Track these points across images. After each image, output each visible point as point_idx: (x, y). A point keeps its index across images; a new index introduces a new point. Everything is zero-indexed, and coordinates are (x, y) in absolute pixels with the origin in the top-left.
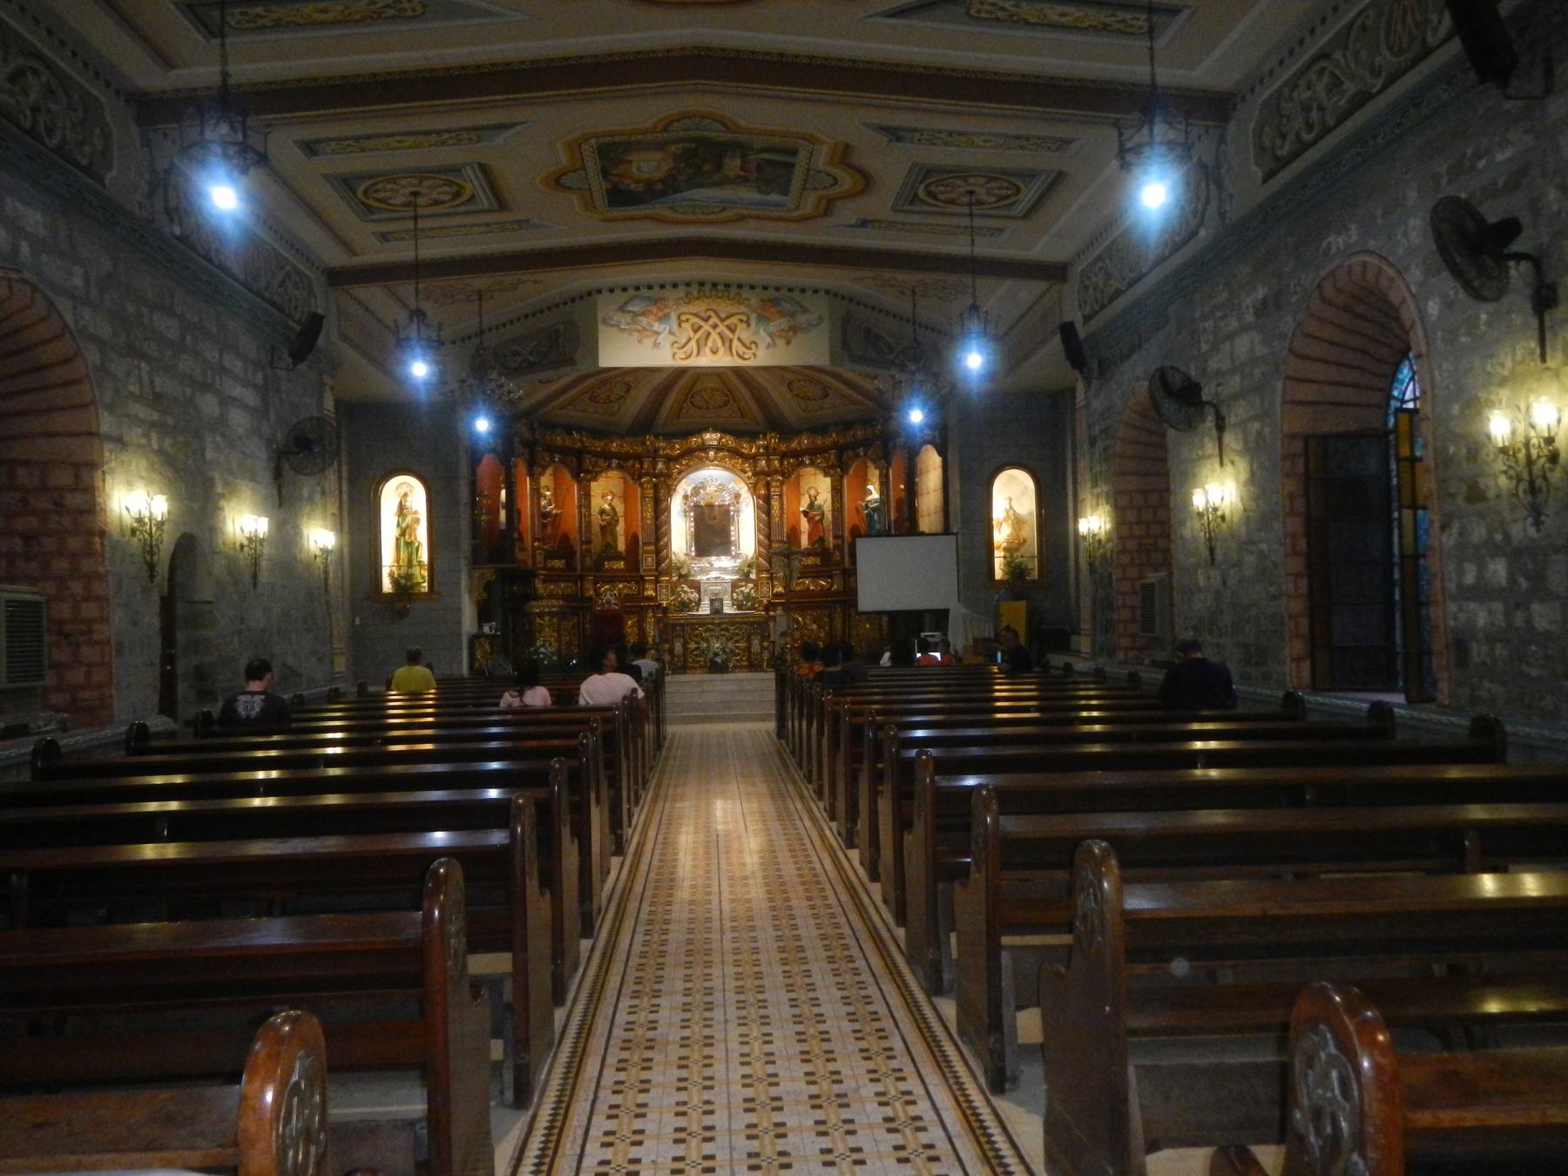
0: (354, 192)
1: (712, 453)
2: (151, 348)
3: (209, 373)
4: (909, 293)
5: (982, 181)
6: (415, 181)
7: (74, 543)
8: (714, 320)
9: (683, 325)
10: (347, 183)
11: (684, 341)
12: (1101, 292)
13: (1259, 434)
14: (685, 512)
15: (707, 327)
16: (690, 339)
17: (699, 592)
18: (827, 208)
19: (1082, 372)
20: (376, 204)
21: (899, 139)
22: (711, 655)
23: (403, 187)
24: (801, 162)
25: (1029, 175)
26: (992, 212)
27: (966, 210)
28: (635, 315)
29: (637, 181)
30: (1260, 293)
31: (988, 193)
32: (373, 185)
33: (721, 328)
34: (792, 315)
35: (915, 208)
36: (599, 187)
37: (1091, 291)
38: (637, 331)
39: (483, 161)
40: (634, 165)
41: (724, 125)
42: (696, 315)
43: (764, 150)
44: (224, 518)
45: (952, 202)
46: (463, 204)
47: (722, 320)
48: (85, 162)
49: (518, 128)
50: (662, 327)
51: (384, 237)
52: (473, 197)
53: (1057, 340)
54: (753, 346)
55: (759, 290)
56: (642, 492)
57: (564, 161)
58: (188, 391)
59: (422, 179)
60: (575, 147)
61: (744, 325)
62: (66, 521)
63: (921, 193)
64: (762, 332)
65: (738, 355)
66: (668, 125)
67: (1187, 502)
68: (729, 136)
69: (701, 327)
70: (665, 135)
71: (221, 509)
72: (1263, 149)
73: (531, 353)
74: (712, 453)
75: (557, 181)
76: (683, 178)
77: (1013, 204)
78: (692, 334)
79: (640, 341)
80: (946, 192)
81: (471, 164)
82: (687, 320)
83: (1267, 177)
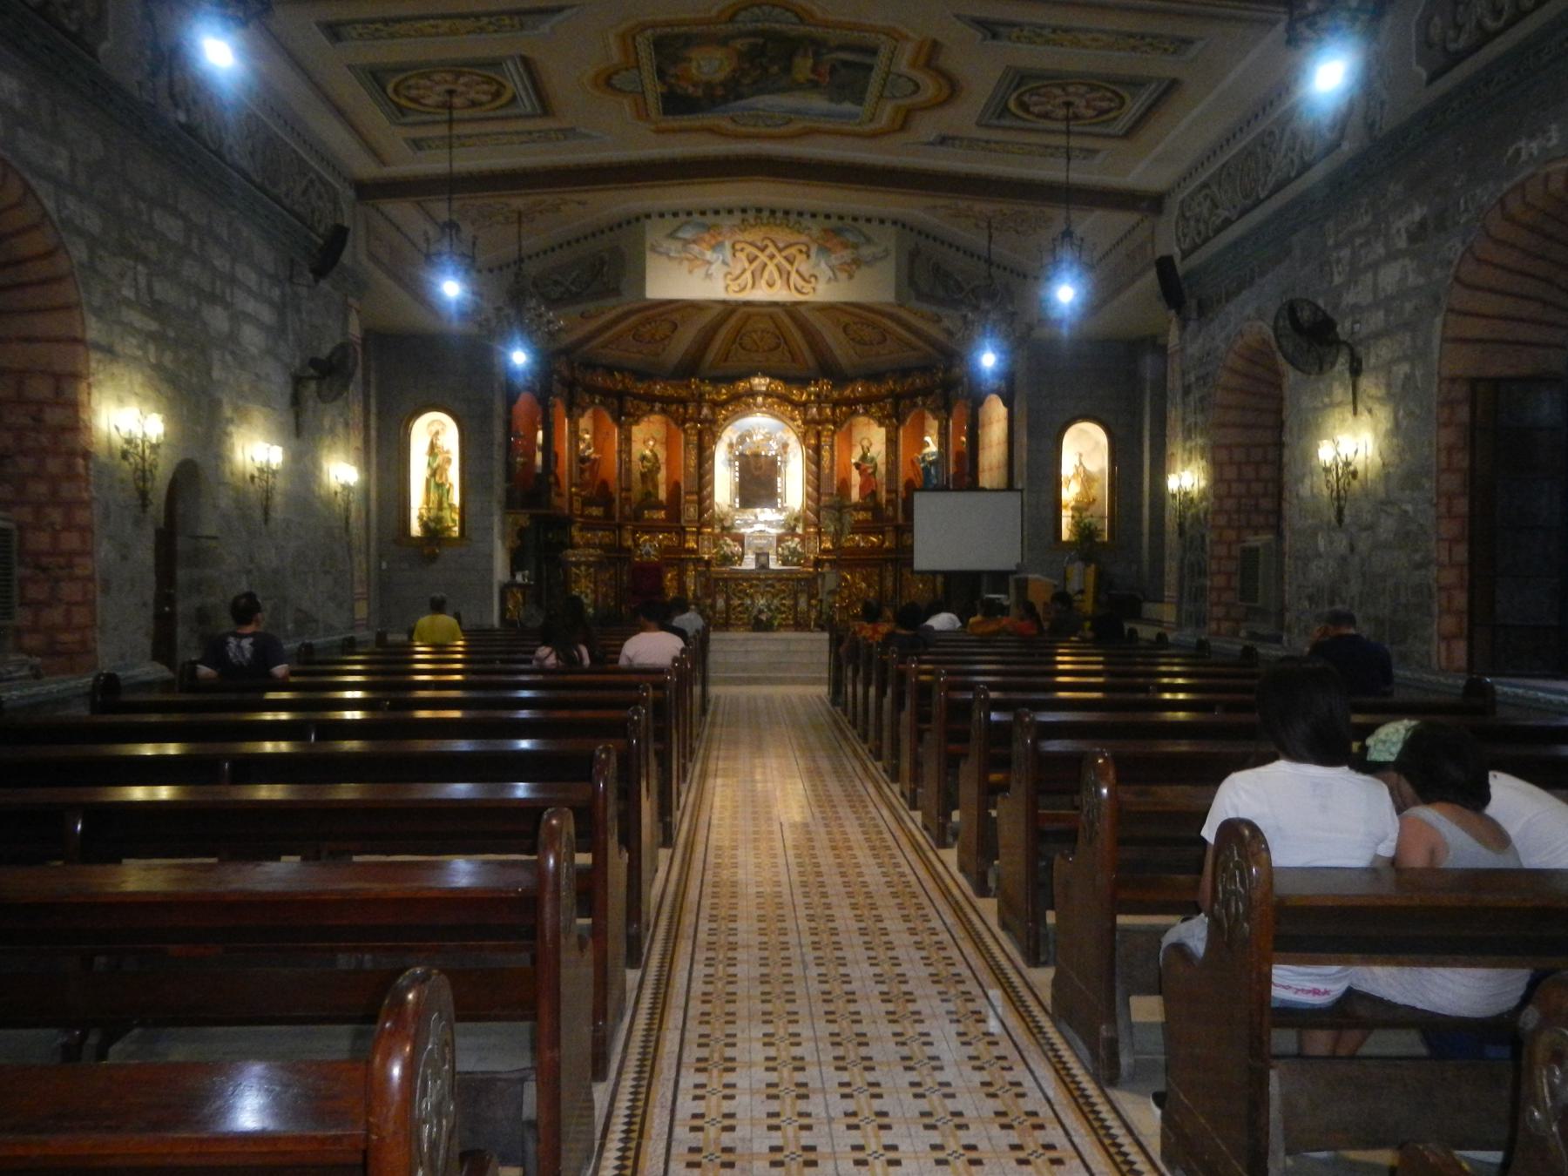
0: (384, 90)
1: (760, 399)
2: (151, 249)
3: (218, 283)
4: (984, 225)
5: (1083, 89)
6: (449, 77)
7: (54, 466)
8: (771, 249)
9: (739, 254)
10: (375, 77)
11: (738, 272)
12: (1206, 223)
13: (1408, 378)
14: (730, 460)
15: (763, 257)
16: (744, 271)
17: (742, 546)
18: (904, 122)
19: (1178, 313)
20: (403, 102)
21: (995, 36)
22: (755, 612)
23: (438, 83)
24: (880, 62)
25: (1136, 84)
26: (1088, 129)
27: (1061, 126)
28: (686, 242)
29: (695, 85)
30: (1418, 213)
31: (1088, 106)
32: (406, 79)
33: (779, 259)
34: (855, 247)
35: (1006, 122)
36: (654, 90)
37: (1192, 223)
38: (688, 259)
39: (527, 53)
40: (694, 64)
41: (797, 15)
42: (752, 244)
43: (842, 48)
44: (233, 444)
45: (1045, 116)
46: (502, 107)
47: (780, 250)
48: (73, 28)
49: (567, 13)
50: (715, 256)
51: (417, 144)
52: (514, 99)
53: (1152, 275)
54: (813, 280)
55: (821, 218)
57: (616, 56)
58: (194, 302)
59: (459, 75)
60: (628, 40)
61: (804, 256)
62: (44, 440)
63: (1012, 105)
64: (823, 265)
65: (796, 289)
66: (735, 14)
67: (1308, 455)
68: (804, 29)
69: (756, 257)
70: (730, 27)
71: (229, 435)
72: (1430, 45)
73: (572, 283)
74: (760, 399)
75: (607, 81)
76: (747, 81)
77: (1115, 119)
78: (746, 264)
79: (691, 272)
80: (1042, 104)
81: (512, 57)
82: (742, 250)
83: (1431, 80)
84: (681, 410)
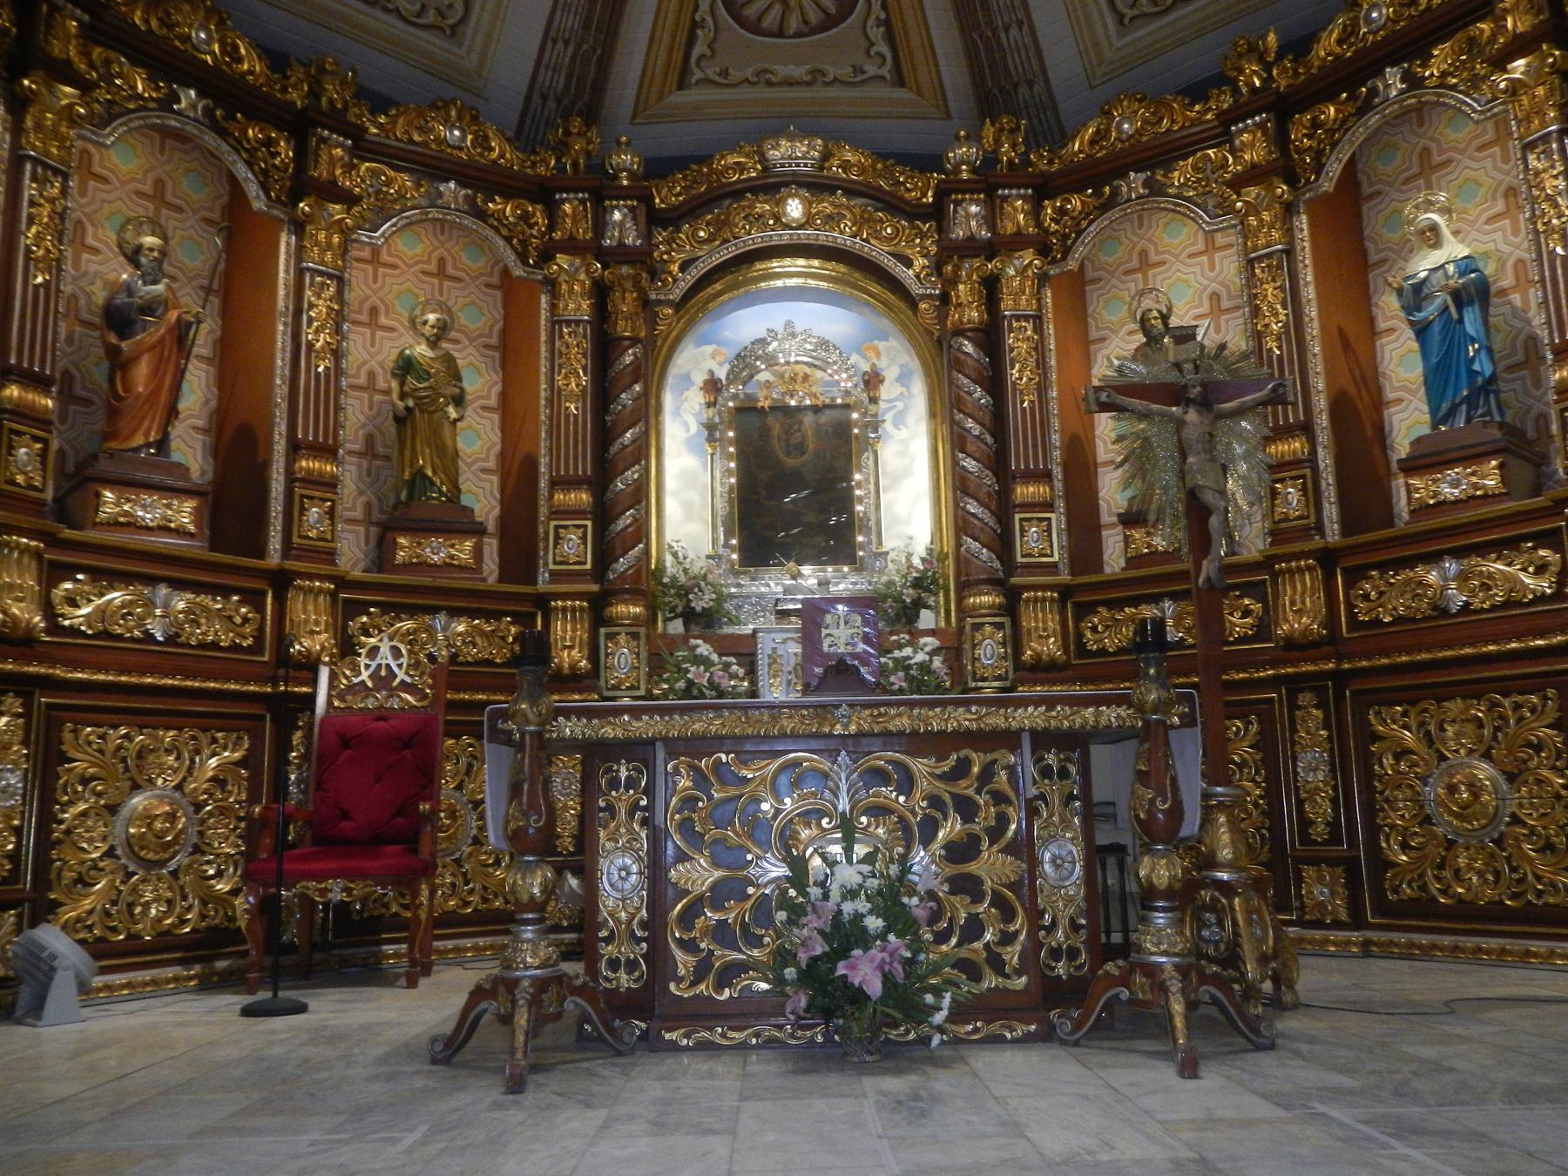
14: (710, 427)
17: (752, 672)
22: (810, 941)
56: (553, 307)
74: (794, 209)
84: (540, 219)
